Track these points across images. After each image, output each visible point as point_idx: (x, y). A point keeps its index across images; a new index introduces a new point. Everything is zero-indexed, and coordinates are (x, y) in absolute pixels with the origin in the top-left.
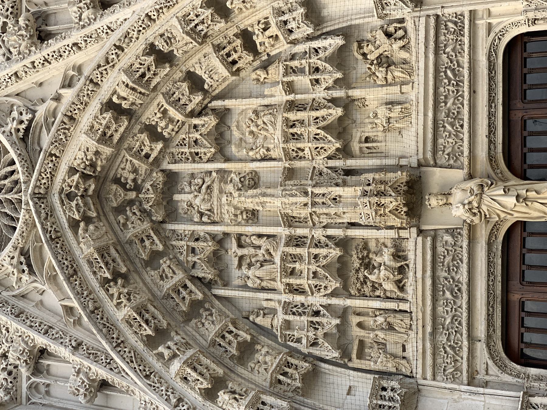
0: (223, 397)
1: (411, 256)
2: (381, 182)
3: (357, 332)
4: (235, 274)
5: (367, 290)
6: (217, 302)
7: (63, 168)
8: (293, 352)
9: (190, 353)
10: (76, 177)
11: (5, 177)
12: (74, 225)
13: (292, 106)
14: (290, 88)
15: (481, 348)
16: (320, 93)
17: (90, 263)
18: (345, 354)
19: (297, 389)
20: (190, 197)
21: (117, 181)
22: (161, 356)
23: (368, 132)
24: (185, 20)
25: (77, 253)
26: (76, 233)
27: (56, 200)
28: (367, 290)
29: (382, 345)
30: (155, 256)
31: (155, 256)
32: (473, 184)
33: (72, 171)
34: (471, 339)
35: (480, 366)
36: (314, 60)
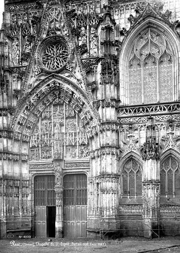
0: (19, 126)
1: (49, 159)
2: (60, 154)
3: (36, 149)
4: (44, 122)
5: (43, 151)
6: (37, 119)
7: (61, 82)
8: (30, 137)
9: (26, 117)
10: (58, 85)
11: (60, 60)
12: (48, 85)
13: (75, 133)
14: (79, 133)
15: (36, 172)
16: (78, 140)
17: (41, 91)
18: (31, 148)
19: (23, 140)
20: (58, 111)
21: (60, 92)
22: (24, 111)
23: (71, 150)
24: (89, 112)
25: (43, 87)
26: (47, 86)
27: (53, 80)
28: (43, 151)
29: (34, 155)
30: (45, 104)
31: (45, 104)
32: (60, 170)
33: (59, 84)
34: (37, 171)
35: (32, 172)
36: (83, 138)
